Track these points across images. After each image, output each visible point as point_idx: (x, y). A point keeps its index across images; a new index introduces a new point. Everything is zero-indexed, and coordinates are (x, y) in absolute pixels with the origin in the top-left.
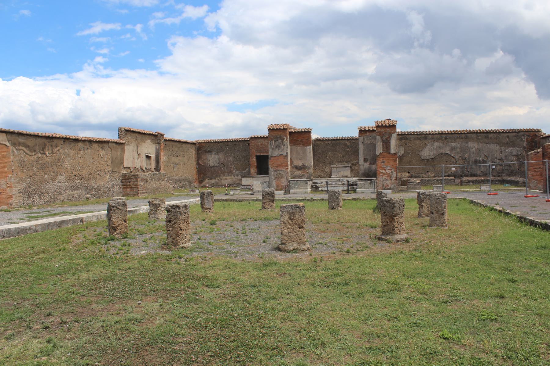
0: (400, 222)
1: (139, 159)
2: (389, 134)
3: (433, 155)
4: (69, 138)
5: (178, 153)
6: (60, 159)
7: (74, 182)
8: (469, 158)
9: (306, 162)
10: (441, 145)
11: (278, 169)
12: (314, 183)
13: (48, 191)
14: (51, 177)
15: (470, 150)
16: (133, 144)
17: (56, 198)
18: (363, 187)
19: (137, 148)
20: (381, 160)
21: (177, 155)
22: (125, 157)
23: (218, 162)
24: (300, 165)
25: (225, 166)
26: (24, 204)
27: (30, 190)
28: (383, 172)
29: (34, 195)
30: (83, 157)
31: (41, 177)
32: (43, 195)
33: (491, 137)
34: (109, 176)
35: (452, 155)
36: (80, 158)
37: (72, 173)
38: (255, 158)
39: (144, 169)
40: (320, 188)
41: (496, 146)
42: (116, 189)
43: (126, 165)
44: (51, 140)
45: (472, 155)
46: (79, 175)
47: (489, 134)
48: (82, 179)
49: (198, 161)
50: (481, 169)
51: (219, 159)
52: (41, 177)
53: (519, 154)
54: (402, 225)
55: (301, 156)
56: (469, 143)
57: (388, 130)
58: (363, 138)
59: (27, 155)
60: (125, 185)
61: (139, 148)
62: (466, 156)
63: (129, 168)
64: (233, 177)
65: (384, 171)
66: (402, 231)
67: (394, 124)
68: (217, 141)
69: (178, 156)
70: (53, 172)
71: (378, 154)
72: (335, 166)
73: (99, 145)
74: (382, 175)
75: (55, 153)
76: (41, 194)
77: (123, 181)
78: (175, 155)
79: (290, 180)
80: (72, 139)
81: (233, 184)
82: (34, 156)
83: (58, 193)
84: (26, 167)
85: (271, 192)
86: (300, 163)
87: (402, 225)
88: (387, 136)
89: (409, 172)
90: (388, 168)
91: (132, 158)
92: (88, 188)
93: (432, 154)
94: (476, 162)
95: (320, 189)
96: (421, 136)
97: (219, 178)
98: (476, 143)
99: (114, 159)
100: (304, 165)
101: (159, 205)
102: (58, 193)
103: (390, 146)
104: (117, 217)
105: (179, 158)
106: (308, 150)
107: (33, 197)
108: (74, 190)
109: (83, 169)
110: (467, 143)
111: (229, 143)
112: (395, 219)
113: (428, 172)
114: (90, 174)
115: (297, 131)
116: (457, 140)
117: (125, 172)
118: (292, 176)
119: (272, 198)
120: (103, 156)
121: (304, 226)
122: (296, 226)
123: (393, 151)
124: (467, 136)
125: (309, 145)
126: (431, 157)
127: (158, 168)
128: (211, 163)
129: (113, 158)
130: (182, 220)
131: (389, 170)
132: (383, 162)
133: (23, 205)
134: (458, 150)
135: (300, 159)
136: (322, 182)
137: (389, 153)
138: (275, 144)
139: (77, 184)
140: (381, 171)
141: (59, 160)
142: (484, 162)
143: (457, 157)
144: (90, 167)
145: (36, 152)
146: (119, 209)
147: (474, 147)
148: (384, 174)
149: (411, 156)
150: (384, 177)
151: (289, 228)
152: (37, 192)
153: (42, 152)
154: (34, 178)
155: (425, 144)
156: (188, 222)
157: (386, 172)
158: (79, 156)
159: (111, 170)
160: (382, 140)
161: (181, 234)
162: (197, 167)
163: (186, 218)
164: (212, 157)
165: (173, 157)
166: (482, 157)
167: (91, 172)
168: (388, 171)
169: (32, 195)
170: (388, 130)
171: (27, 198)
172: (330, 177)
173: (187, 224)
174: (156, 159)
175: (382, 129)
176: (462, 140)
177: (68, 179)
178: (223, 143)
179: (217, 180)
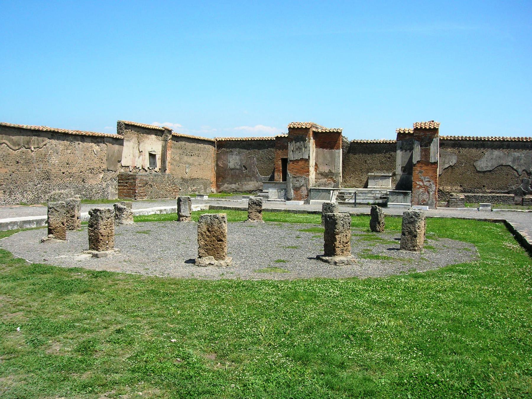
0: (343, 242)
1: (141, 158)
3: (492, 166)
4: (58, 131)
5: (192, 151)
6: (47, 154)
7: (61, 180)
9: (334, 168)
10: (502, 154)
11: (298, 175)
12: (340, 193)
13: (31, 189)
14: (36, 174)
16: (133, 140)
17: (41, 197)
18: (395, 201)
19: (139, 145)
21: (191, 154)
22: (123, 154)
23: (240, 164)
24: (327, 171)
25: (246, 169)
26: (4, 201)
27: (12, 187)
28: (420, 184)
29: (16, 192)
30: (73, 153)
31: (25, 173)
32: (26, 193)
34: (103, 175)
35: (515, 168)
36: (70, 153)
37: (60, 170)
38: (280, 161)
39: (147, 169)
40: (347, 200)
42: (111, 190)
43: (124, 163)
44: (38, 134)
46: (67, 173)
48: (71, 177)
49: (217, 162)
51: (240, 161)
52: (25, 173)
54: (345, 245)
55: (328, 161)
57: (428, 133)
58: (402, 143)
59: (10, 149)
60: (122, 186)
61: (141, 145)
63: (128, 167)
64: (255, 182)
65: (421, 183)
66: (345, 252)
67: (435, 126)
68: (239, 139)
69: (191, 155)
70: (38, 168)
71: (414, 161)
72: (373, 174)
73: (93, 139)
74: (419, 188)
75: (41, 148)
76: (24, 192)
77: (119, 181)
78: (189, 154)
79: (311, 189)
80: (61, 133)
81: (256, 191)
82: (18, 151)
83: (43, 191)
84: (9, 162)
85: (258, 201)
86: (326, 169)
87: (345, 245)
89: (461, 186)
91: (131, 156)
92: (78, 188)
93: (490, 164)
95: (347, 201)
96: (477, 143)
97: (239, 183)
99: (110, 156)
100: (330, 172)
101: (125, 209)
102: (43, 191)
103: (430, 153)
104: (54, 219)
105: (192, 157)
106: (337, 155)
107: (15, 194)
108: (61, 188)
109: (73, 167)
111: (253, 142)
112: (337, 238)
113: (484, 186)
114: (81, 172)
115: (324, 131)
117: (122, 170)
118: (316, 184)
119: (258, 208)
120: (96, 152)
121: (223, 239)
122: (214, 238)
125: (338, 148)
126: (488, 169)
127: (163, 169)
128: (231, 165)
129: (108, 155)
130: (104, 225)
131: (427, 182)
133: (3, 202)
134: (522, 161)
135: (327, 165)
136: (350, 193)
138: (295, 146)
139: (65, 182)
141: (45, 155)
143: (520, 170)
144: (81, 165)
145: (20, 146)
146: (57, 210)
148: (421, 187)
149: (464, 166)
150: (421, 190)
151: (206, 240)
152: (20, 190)
153: (26, 146)
154: (17, 174)
155: (483, 152)
156: (111, 228)
157: (424, 185)
158: (69, 151)
159: (106, 169)
161: (101, 240)
162: (216, 168)
163: (109, 224)
164: (233, 158)
165: (186, 157)
167: (82, 170)
169: (14, 192)
170: (428, 134)
171: (8, 195)
172: (367, 188)
173: (110, 230)
174: (162, 158)
175: (422, 133)
177: (55, 177)
178: (246, 142)
179: (237, 185)
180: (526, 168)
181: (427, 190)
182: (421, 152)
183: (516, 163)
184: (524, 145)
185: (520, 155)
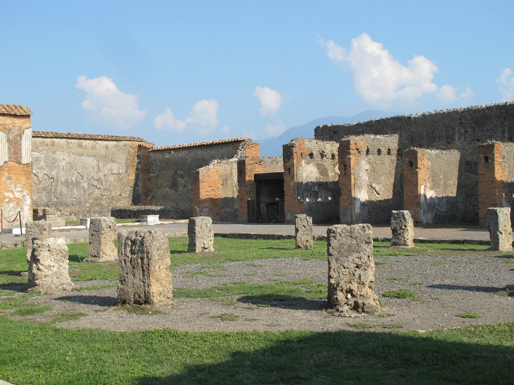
2: (19, 129)
8: (57, 177)
15: (58, 165)
20: (6, 174)
28: (10, 196)
33: (86, 146)
41: (92, 160)
45: (62, 173)
47: (83, 141)
50: (74, 194)
53: (121, 173)
56: (58, 153)
57: (17, 122)
62: (53, 173)
65: (11, 195)
74: (8, 202)
90: (19, 189)
94: (67, 184)
98: (67, 154)
110: (54, 153)
116: (41, 148)
124: (54, 142)
131: (19, 194)
132: (10, 178)
137: (20, 163)
140: (6, 194)
142: (78, 183)
143: (40, 175)
147: (64, 159)
148: (11, 200)
150: (11, 205)
157: (15, 197)
160: (8, 140)
166: (74, 176)
168: (17, 195)
170: (18, 122)
176: (47, 148)
180: (47, 172)
183: (35, 167)
184: (43, 142)
185: (39, 156)
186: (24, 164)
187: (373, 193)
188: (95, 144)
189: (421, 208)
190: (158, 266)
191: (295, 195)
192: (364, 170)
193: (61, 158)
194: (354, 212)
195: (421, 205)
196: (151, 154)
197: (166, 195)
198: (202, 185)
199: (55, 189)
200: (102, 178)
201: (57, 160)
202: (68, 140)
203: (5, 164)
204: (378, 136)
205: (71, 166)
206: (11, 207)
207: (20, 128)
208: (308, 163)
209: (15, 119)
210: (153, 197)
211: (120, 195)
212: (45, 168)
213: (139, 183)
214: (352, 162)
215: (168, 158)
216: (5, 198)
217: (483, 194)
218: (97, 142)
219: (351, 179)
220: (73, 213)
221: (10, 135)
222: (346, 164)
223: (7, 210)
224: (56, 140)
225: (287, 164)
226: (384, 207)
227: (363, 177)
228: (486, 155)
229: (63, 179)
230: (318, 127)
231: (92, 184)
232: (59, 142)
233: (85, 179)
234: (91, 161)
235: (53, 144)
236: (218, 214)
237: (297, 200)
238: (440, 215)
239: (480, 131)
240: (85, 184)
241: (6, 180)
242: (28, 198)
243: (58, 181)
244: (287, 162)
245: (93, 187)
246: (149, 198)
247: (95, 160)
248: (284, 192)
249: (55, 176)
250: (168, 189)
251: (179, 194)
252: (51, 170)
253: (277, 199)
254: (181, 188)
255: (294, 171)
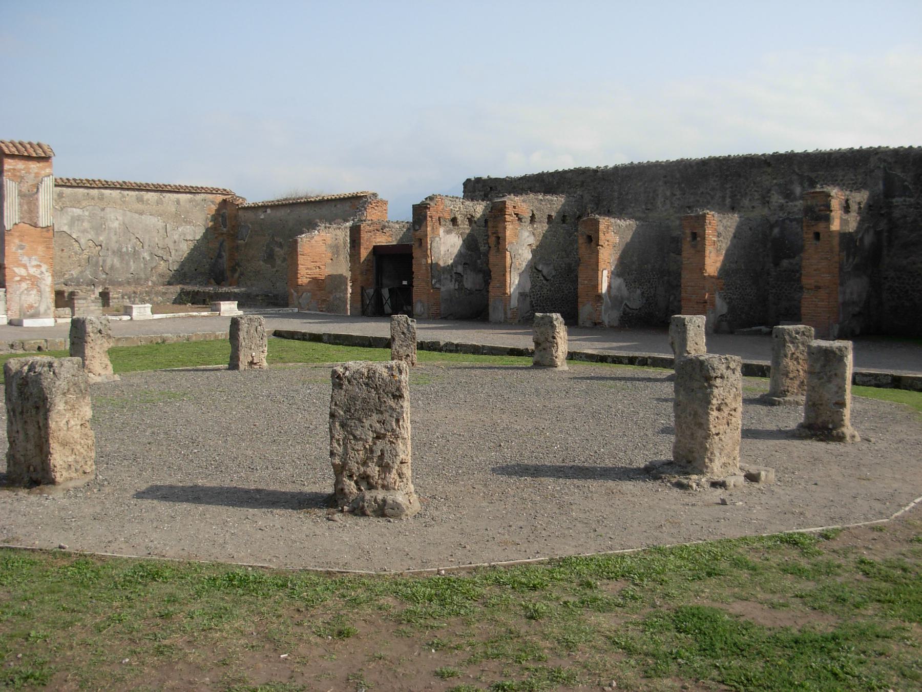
2: (35, 177)
20: (17, 241)
33: (148, 200)
50: (131, 268)
56: (108, 210)
57: (32, 166)
62: (101, 238)
65: (22, 272)
88: (31, 183)
90: (34, 263)
98: (121, 211)
110: (103, 209)
116: (84, 203)
123: (43, 221)
124: (102, 195)
131: (35, 269)
132: (21, 247)
137: (36, 226)
140: (16, 270)
143: (83, 241)
147: (117, 219)
148: (23, 279)
150: (24, 285)
157: (28, 273)
160: (20, 191)
168: (32, 271)
170: (34, 166)
180: (92, 236)
181: (34, 282)
182: (21, 205)
184: (88, 194)
185: (81, 213)
186: (42, 228)
187: (538, 277)
188: (161, 197)
189: (602, 303)
190: (64, 422)
191: (428, 278)
192: (526, 245)
193: (113, 217)
194: (510, 305)
195: (603, 299)
196: (241, 213)
197: (259, 272)
198: (301, 259)
199: (104, 261)
200: (171, 246)
201: (107, 219)
202: (122, 192)
203: (15, 226)
204: (549, 197)
205: (126, 228)
206: (23, 289)
207: (37, 175)
208: (448, 232)
209: (30, 163)
210: (242, 274)
211: (196, 270)
212: (89, 230)
213: (223, 254)
214: (508, 233)
215: (262, 219)
216: (15, 274)
217: (688, 286)
218: (164, 194)
219: (505, 257)
220: (126, 295)
221: (22, 185)
222: (500, 235)
223: (18, 292)
224: (107, 192)
225: (418, 233)
226: (554, 299)
227: (524, 255)
228: (695, 231)
229: (115, 246)
230: (468, 180)
231: (156, 254)
232: (111, 194)
233: (146, 247)
234: (155, 222)
235: (101, 198)
236: (324, 300)
237: (430, 285)
238: (630, 313)
239: (692, 194)
240: (145, 254)
241: (17, 250)
242: (48, 276)
243: (108, 250)
244: (418, 230)
245: (157, 258)
246: (237, 275)
247: (160, 221)
248: (413, 273)
249: (104, 242)
250: (262, 263)
251: (277, 271)
252: (98, 234)
253: (405, 283)
254: (279, 262)
255: (427, 243)
